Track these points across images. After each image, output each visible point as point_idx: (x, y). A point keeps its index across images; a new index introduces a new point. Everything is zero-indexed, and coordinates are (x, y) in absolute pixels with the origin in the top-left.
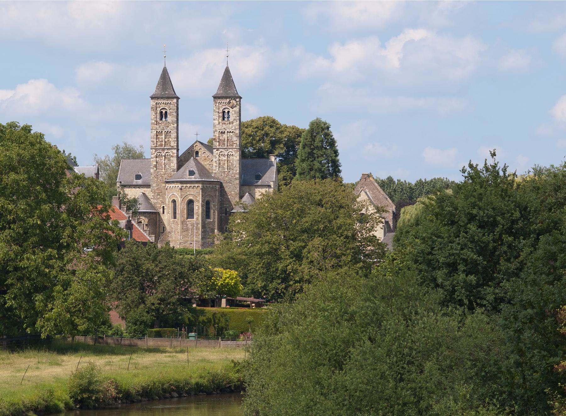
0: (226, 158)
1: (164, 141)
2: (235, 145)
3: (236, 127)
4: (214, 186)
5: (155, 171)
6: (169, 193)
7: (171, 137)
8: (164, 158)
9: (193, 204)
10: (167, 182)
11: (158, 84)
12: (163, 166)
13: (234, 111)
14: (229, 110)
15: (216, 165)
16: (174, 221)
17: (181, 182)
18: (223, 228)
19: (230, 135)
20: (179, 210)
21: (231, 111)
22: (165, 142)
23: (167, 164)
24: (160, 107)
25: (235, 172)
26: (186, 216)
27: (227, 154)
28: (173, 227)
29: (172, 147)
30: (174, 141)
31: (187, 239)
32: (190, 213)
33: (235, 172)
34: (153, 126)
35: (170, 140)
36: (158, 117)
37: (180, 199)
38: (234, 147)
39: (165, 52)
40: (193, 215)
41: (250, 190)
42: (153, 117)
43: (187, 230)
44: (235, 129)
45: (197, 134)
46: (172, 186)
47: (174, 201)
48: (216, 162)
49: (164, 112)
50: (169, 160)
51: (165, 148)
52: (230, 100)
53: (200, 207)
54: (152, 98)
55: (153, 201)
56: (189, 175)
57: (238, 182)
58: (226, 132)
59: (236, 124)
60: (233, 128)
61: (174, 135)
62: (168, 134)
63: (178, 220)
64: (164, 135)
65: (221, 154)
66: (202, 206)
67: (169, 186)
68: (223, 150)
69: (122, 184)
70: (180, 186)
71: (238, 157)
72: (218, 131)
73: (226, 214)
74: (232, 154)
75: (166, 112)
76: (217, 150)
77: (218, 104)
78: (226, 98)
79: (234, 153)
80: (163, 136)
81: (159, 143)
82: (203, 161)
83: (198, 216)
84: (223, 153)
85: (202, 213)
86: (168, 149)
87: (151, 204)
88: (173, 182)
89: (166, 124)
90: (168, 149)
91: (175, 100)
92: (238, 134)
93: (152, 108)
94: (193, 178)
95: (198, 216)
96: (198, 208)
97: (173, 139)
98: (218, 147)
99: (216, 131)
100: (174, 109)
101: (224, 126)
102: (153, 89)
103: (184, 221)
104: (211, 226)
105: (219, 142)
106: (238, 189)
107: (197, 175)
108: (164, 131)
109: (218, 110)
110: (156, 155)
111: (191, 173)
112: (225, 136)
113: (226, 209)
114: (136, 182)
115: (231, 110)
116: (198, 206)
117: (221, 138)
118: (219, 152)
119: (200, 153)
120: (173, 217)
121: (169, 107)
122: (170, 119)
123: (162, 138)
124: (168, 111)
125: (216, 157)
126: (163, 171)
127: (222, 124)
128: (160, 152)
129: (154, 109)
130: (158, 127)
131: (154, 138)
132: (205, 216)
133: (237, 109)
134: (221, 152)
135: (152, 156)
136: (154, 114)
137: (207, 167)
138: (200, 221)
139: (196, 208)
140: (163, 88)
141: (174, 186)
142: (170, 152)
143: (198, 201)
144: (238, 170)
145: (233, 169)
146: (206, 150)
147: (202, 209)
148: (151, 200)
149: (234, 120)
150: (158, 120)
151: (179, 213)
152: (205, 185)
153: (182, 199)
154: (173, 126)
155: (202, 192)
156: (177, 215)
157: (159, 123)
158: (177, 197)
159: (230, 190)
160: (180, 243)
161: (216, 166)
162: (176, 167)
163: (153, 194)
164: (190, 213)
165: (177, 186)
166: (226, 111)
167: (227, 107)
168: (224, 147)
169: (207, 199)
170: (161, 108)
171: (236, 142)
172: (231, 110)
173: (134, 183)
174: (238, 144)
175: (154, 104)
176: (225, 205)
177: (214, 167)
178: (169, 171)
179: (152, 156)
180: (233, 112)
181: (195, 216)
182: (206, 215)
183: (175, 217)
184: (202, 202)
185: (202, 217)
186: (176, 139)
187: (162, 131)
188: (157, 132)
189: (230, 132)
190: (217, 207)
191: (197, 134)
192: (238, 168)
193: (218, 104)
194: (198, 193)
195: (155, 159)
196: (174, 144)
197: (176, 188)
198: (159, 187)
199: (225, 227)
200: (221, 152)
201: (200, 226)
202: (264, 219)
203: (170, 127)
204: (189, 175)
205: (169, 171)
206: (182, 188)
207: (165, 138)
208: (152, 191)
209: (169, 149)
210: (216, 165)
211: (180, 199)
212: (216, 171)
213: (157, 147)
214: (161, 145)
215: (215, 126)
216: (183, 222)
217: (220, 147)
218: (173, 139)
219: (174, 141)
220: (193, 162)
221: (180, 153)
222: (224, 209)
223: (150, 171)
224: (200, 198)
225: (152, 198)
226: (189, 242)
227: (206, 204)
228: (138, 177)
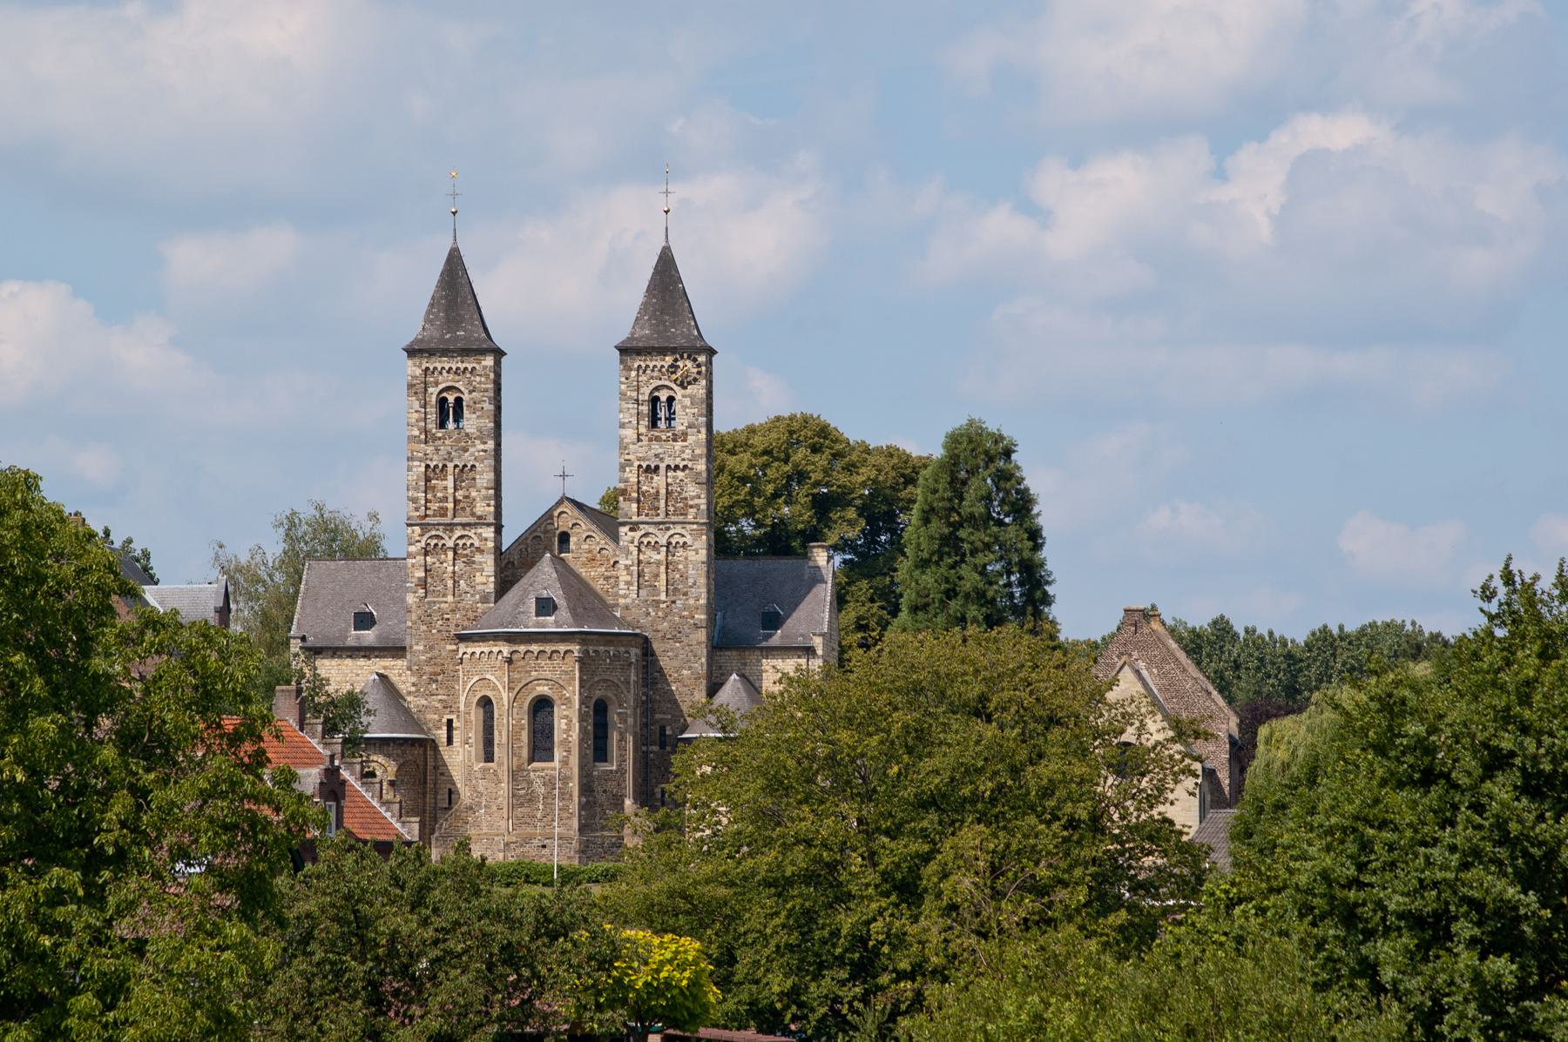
0: (663, 554)
1: (451, 499)
2: (693, 511)
3: (698, 451)
4: (622, 649)
5: (421, 599)
6: (468, 674)
7: (474, 486)
8: (450, 554)
9: (552, 716)
10: (463, 638)
11: (432, 305)
12: (450, 583)
13: (691, 397)
14: (672, 394)
15: (628, 578)
16: (484, 770)
17: (510, 638)
18: (654, 794)
19: (674, 477)
20: (504, 734)
21: (678, 397)
22: (456, 502)
23: (461, 577)
24: (437, 384)
25: (691, 602)
26: (525, 753)
27: (664, 542)
28: (481, 789)
29: (480, 517)
30: (486, 498)
31: (529, 830)
32: (541, 744)
33: (691, 602)
34: (416, 446)
35: (474, 494)
36: (433, 416)
38: (690, 518)
39: (455, 195)
40: (551, 750)
41: (745, 664)
42: (416, 415)
43: (531, 799)
44: (694, 458)
45: (564, 476)
46: (478, 651)
47: (486, 703)
48: (627, 567)
49: (451, 399)
50: (470, 563)
51: (457, 520)
52: (676, 360)
53: (575, 721)
54: (412, 352)
55: (413, 702)
56: (538, 614)
57: (702, 635)
58: (663, 466)
59: (697, 442)
60: (687, 454)
61: (485, 478)
62: (464, 474)
63: (500, 764)
64: (451, 478)
65: (645, 540)
66: (582, 719)
67: (470, 650)
68: (651, 529)
69: (309, 644)
70: (506, 650)
71: (704, 552)
72: (636, 464)
73: (663, 745)
74: (681, 540)
75: (459, 401)
76: (631, 530)
77: (634, 373)
78: (663, 351)
79: (688, 539)
80: (450, 483)
81: (434, 506)
82: (584, 565)
83: (568, 751)
84: (652, 539)
85: (581, 741)
86: (464, 525)
87: (407, 712)
88: (483, 638)
89: (458, 441)
90: (464, 525)
91: (489, 361)
92: (704, 475)
93: (410, 386)
94: (549, 624)
95: (568, 751)
96: (567, 724)
97: (484, 492)
98: (635, 518)
99: (629, 463)
100: (486, 390)
101: (657, 448)
102: (413, 326)
103: (520, 769)
104: (611, 786)
105: (638, 501)
106: (703, 660)
107: (564, 612)
108: (450, 466)
109: (635, 394)
111: (545, 607)
112: (659, 481)
113: (663, 729)
114: (354, 637)
115: (679, 393)
116: (566, 717)
117: (644, 488)
118: (638, 534)
119: (573, 540)
120: (482, 753)
121: (470, 383)
122: (471, 422)
123: (446, 488)
124: (466, 397)
125: (628, 553)
126: (450, 598)
127: (650, 440)
128: (437, 537)
129: (417, 389)
130: (430, 449)
131: (417, 489)
132: (590, 752)
133: (698, 389)
134: (646, 535)
135: (413, 549)
136: (416, 405)
137: (599, 585)
138: (576, 770)
139: (560, 725)
140: (447, 317)
141: (486, 650)
142: (473, 536)
143: (568, 701)
144: (704, 595)
145: (685, 594)
146: (594, 527)
147: (583, 730)
148: (409, 699)
149: (690, 426)
150: (432, 426)
151: (504, 740)
152: (591, 649)
153: (512, 695)
154: (482, 447)
155: (581, 671)
156: (496, 749)
157: (435, 439)
158: (495, 688)
159: (676, 663)
160: (507, 844)
161: (628, 583)
162: (492, 586)
163: (414, 679)
164: (541, 744)
165: (495, 650)
166: (663, 398)
167: (667, 383)
168: (657, 519)
169: (598, 694)
170: (441, 387)
171: (696, 501)
172: (679, 393)
173: (350, 642)
174: (703, 507)
175: (418, 372)
176: (658, 716)
177: (622, 585)
178: (469, 600)
179: (413, 549)
180: (687, 402)
181: (558, 754)
182: (596, 749)
183: (489, 757)
184: (582, 703)
185: (582, 756)
186: (492, 492)
187: (445, 466)
188: (427, 466)
189: (677, 468)
190: (630, 721)
191: (564, 476)
192: (704, 590)
193: (634, 373)
194: (566, 673)
195: (420, 558)
196: (484, 508)
197: (493, 656)
198: (436, 652)
199: (658, 790)
200: (646, 535)
201: (574, 786)
202: (791, 763)
203: (472, 450)
204: (538, 614)
205: (469, 600)
206: (515, 657)
207: (456, 489)
208: (409, 669)
209: (469, 525)
210: (628, 578)
211: (505, 695)
212: (628, 601)
213: (428, 520)
214: (443, 512)
215: (623, 447)
216: (516, 775)
217: (642, 518)
218: (484, 492)
219: (486, 498)
220: (553, 570)
221: (508, 540)
222: (655, 728)
223: (403, 600)
224: (573, 692)
225: (409, 693)
226: (536, 842)
227: (596, 711)
228: (364, 620)
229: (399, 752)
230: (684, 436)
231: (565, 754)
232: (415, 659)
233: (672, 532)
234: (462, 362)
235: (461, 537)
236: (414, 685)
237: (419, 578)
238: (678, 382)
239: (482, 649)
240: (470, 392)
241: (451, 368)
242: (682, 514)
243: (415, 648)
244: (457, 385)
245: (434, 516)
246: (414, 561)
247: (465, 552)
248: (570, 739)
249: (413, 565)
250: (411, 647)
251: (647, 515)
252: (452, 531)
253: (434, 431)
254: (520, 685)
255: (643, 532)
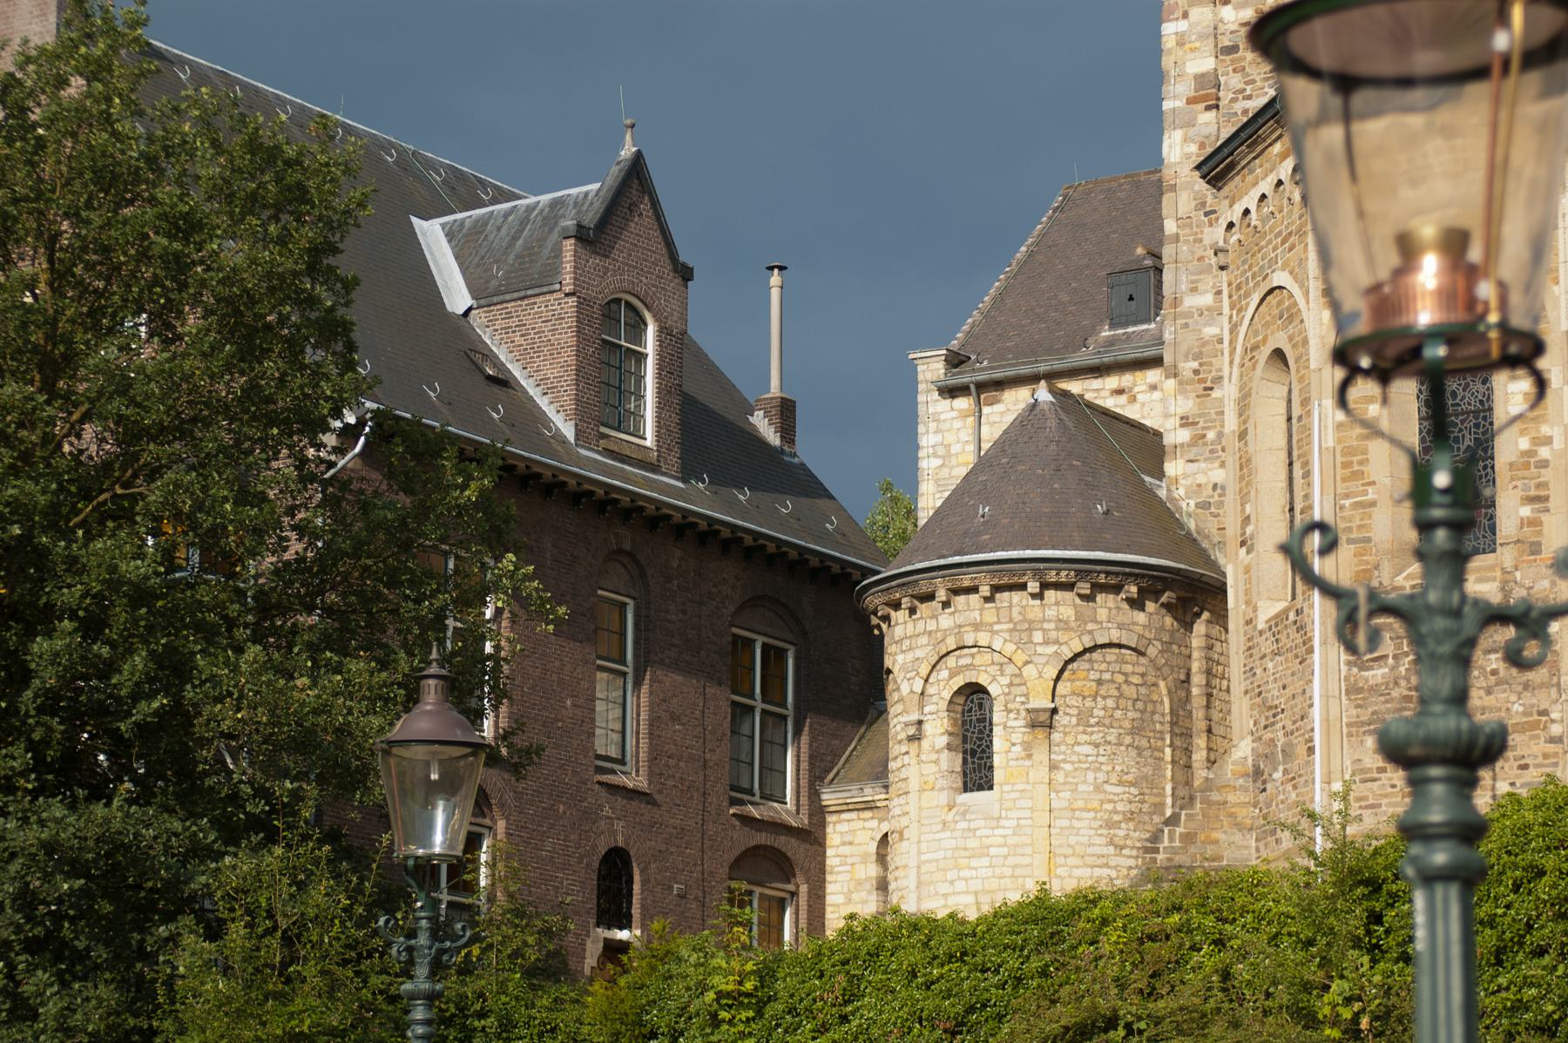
28: (1274, 693)
46: (1250, 201)
163: (1186, 405)
229: (1068, 612)
231: (1526, 511)
232: (1188, 341)
236: (1186, 422)
237: (1200, 79)
243: (1190, 302)
246: (1182, 25)
248: (1544, 452)
249: (1181, 41)
250: (1176, 302)
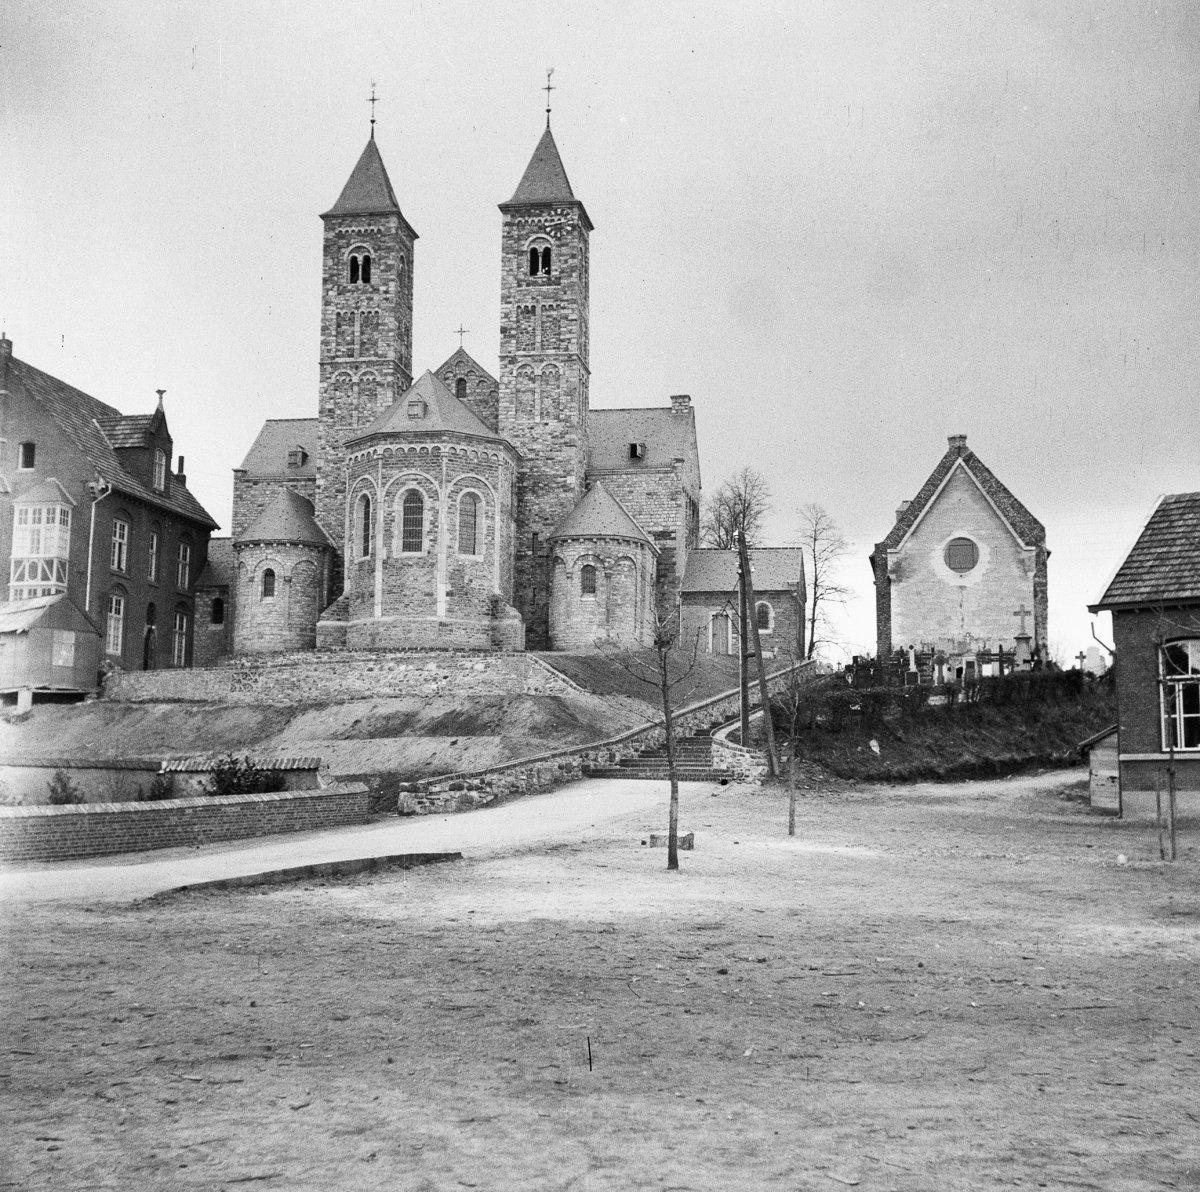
22: (363, 344)
24: (348, 245)
29: (381, 356)
37: (381, 493)
45: (461, 332)
76: (510, 362)
80: (357, 328)
81: (343, 349)
84: (528, 370)
86: (369, 363)
93: (326, 248)
110: (333, 380)
123: (353, 332)
124: (373, 255)
129: (329, 248)
165: (371, 450)
170: (351, 248)
191: (461, 332)
207: (362, 333)
213: (337, 360)
230: (557, 281)
233: (545, 363)
234: (369, 225)
235: (364, 374)
238: (552, 234)
239: (363, 452)
240: (375, 251)
241: (360, 231)
242: (554, 348)
244: (365, 245)
245: (343, 356)
247: (369, 387)
251: (524, 349)
252: (357, 368)
253: (345, 285)
254: (392, 481)
255: (520, 364)
